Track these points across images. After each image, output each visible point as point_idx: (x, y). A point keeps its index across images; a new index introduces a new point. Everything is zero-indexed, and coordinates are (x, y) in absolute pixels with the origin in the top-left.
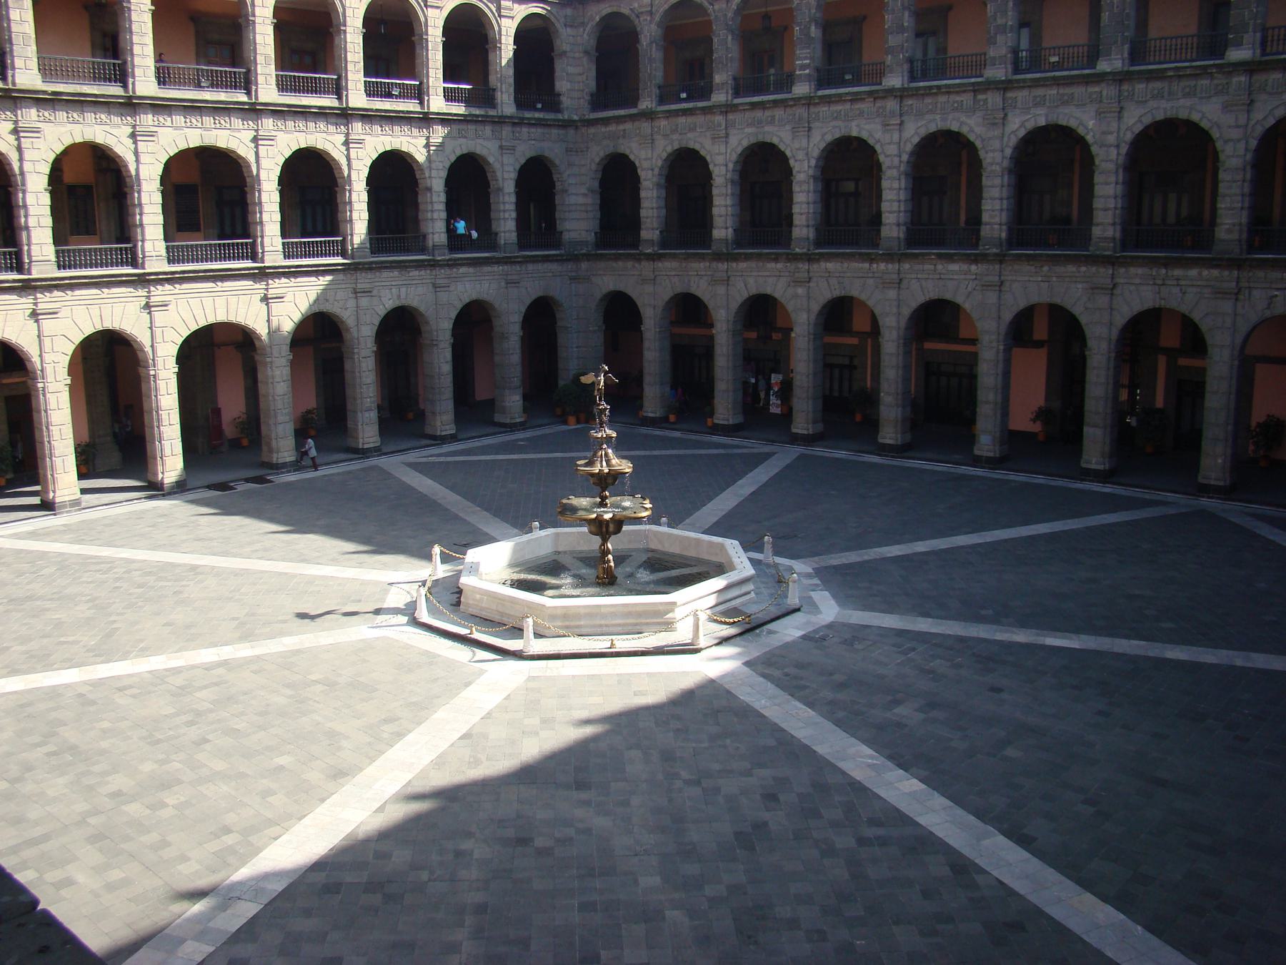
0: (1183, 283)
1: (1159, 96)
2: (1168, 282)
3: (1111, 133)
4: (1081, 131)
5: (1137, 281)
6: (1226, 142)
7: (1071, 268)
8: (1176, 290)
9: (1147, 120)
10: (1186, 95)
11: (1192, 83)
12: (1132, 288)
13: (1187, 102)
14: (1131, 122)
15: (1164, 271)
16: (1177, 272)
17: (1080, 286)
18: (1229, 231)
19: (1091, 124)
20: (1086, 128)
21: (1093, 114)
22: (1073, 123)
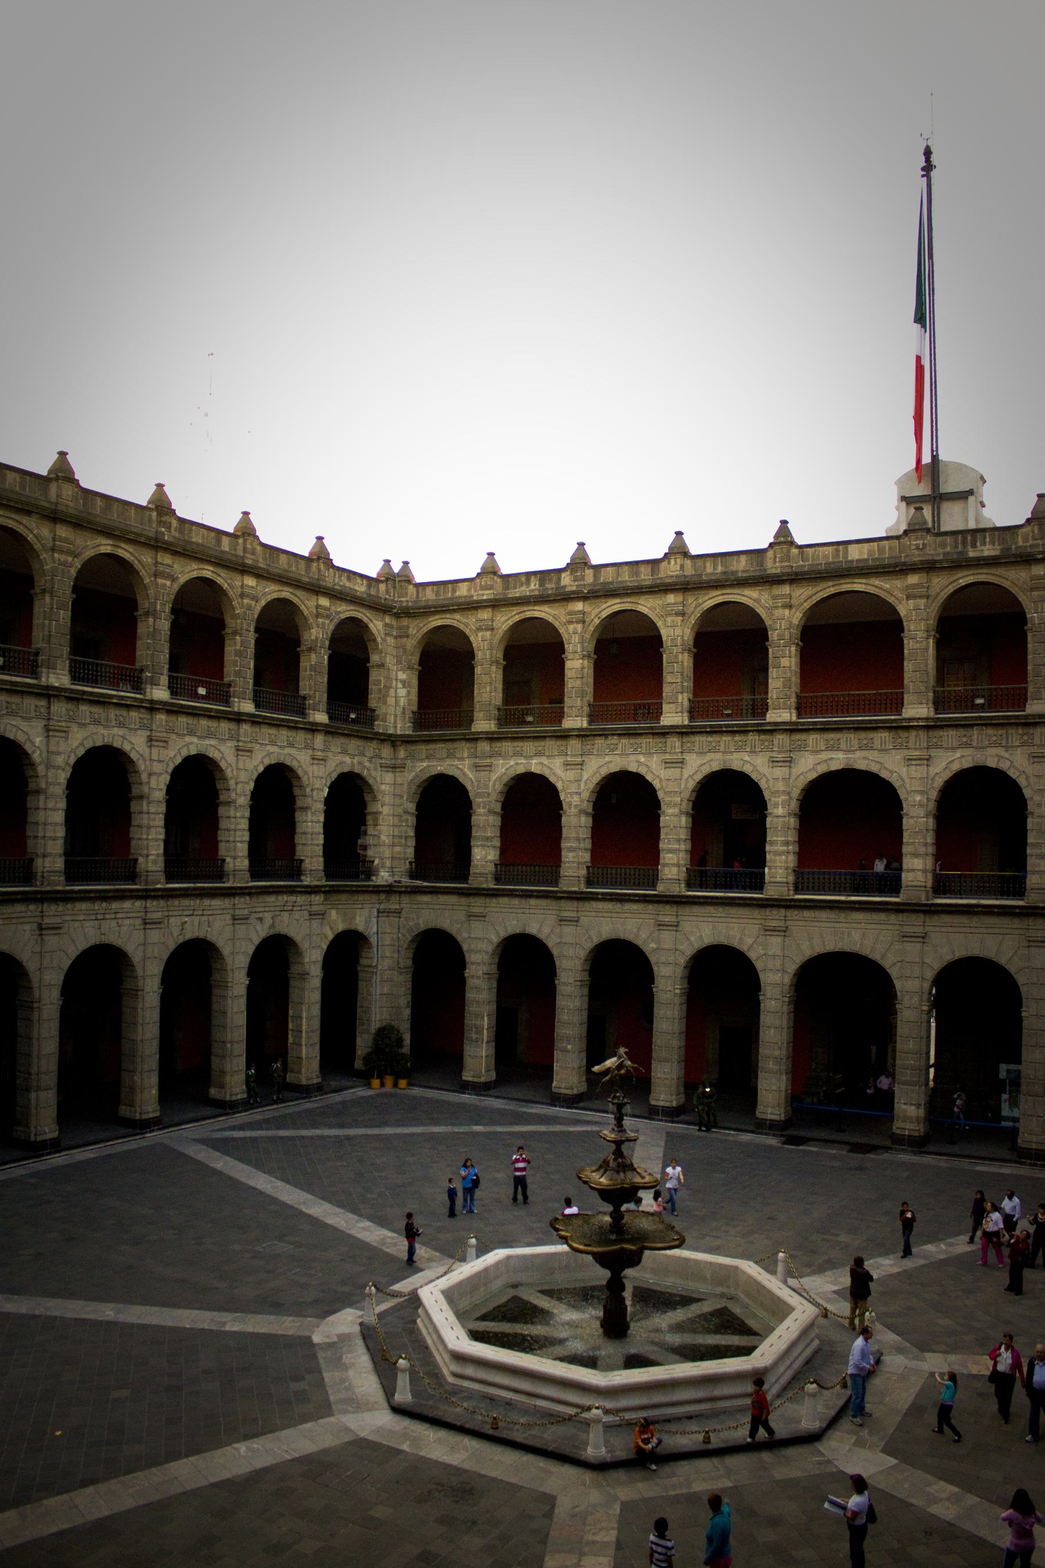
0: (118, 916)
1: (97, 722)
2: (108, 916)
3: (59, 754)
4: (28, 747)
5: (81, 918)
6: (150, 775)
7: (20, 908)
8: (114, 923)
9: (89, 745)
10: (121, 725)
11: (124, 713)
12: (77, 924)
13: (121, 732)
14: (75, 744)
15: (104, 904)
16: (115, 905)
17: (27, 927)
18: (155, 862)
19: (38, 740)
20: (33, 743)
21: (40, 730)
22: (20, 738)
